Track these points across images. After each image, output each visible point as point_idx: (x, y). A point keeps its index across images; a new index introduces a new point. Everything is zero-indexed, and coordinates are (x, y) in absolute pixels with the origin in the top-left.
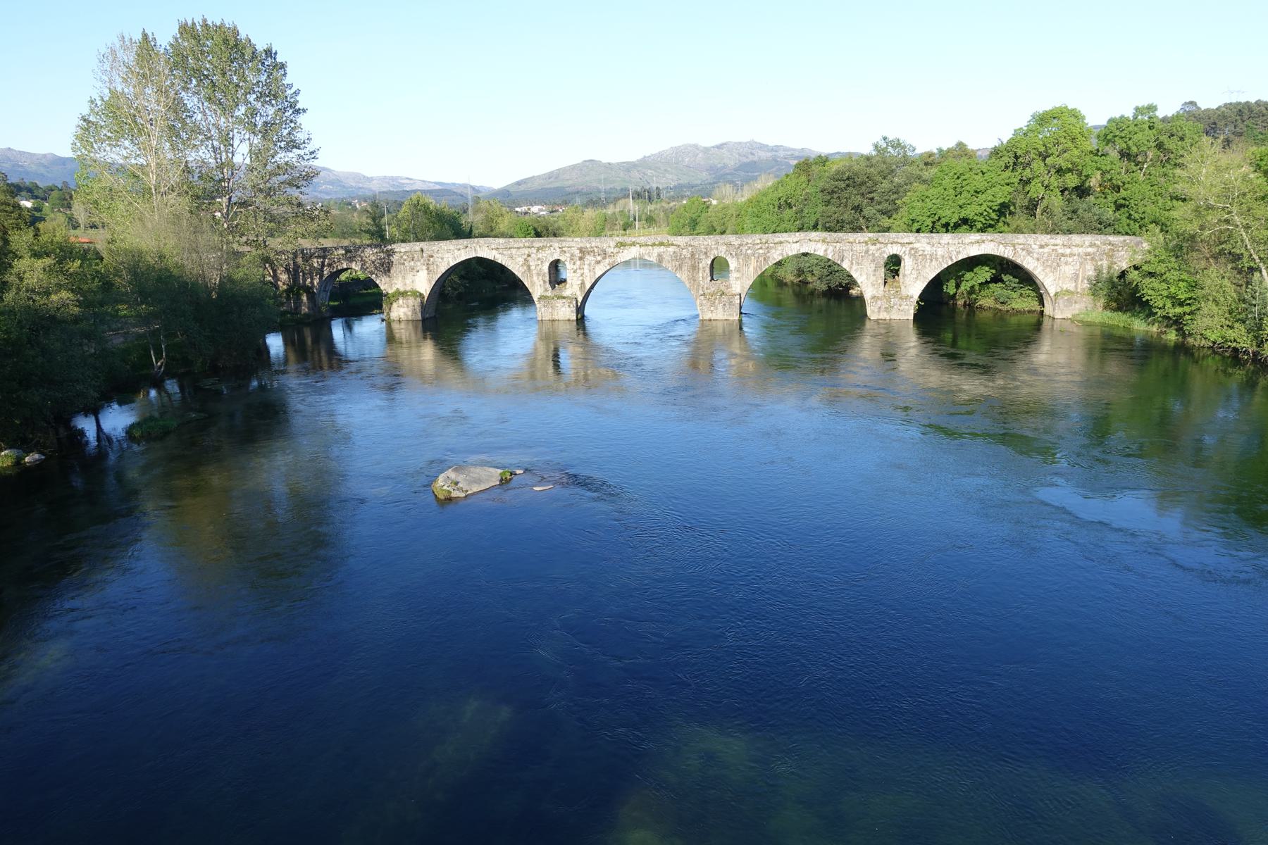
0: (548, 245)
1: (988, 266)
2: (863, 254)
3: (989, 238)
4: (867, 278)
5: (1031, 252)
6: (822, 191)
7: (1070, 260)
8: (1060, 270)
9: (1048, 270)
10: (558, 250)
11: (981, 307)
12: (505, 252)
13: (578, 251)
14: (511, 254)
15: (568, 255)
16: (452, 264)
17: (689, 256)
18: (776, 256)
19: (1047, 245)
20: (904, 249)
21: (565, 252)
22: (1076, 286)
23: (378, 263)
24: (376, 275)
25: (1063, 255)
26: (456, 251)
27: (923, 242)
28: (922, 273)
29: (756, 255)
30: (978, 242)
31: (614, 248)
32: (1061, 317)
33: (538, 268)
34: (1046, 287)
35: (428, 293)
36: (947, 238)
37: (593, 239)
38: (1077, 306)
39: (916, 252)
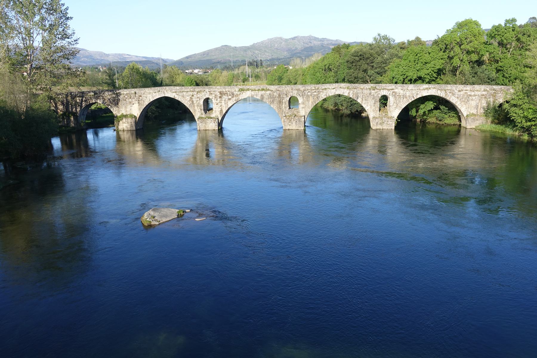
0: (203, 90)
1: (432, 101)
2: (368, 95)
3: (433, 87)
4: (370, 107)
5: (454, 94)
6: (347, 62)
7: (474, 98)
8: (469, 103)
9: (463, 103)
10: (208, 93)
11: (429, 122)
12: (180, 94)
13: (219, 94)
14: (183, 95)
15: (213, 95)
16: (152, 100)
17: (277, 96)
18: (323, 96)
19: (462, 91)
20: (389, 92)
21: (212, 94)
22: (477, 111)
23: (112, 100)
24: (111, 106)
25: (470, 95)
26: (154, 93)
27: (399, 89)
28: (399, 105)
29: (313, 96)
30: (427, 89)
31: (238, 92)
32: (470, 128)
33: (198, 102)
34: (462, 112)
35: (139, 115)
36: (411, 86)
37: (227, 87)
38: (478, 122)
39: (395, 94)
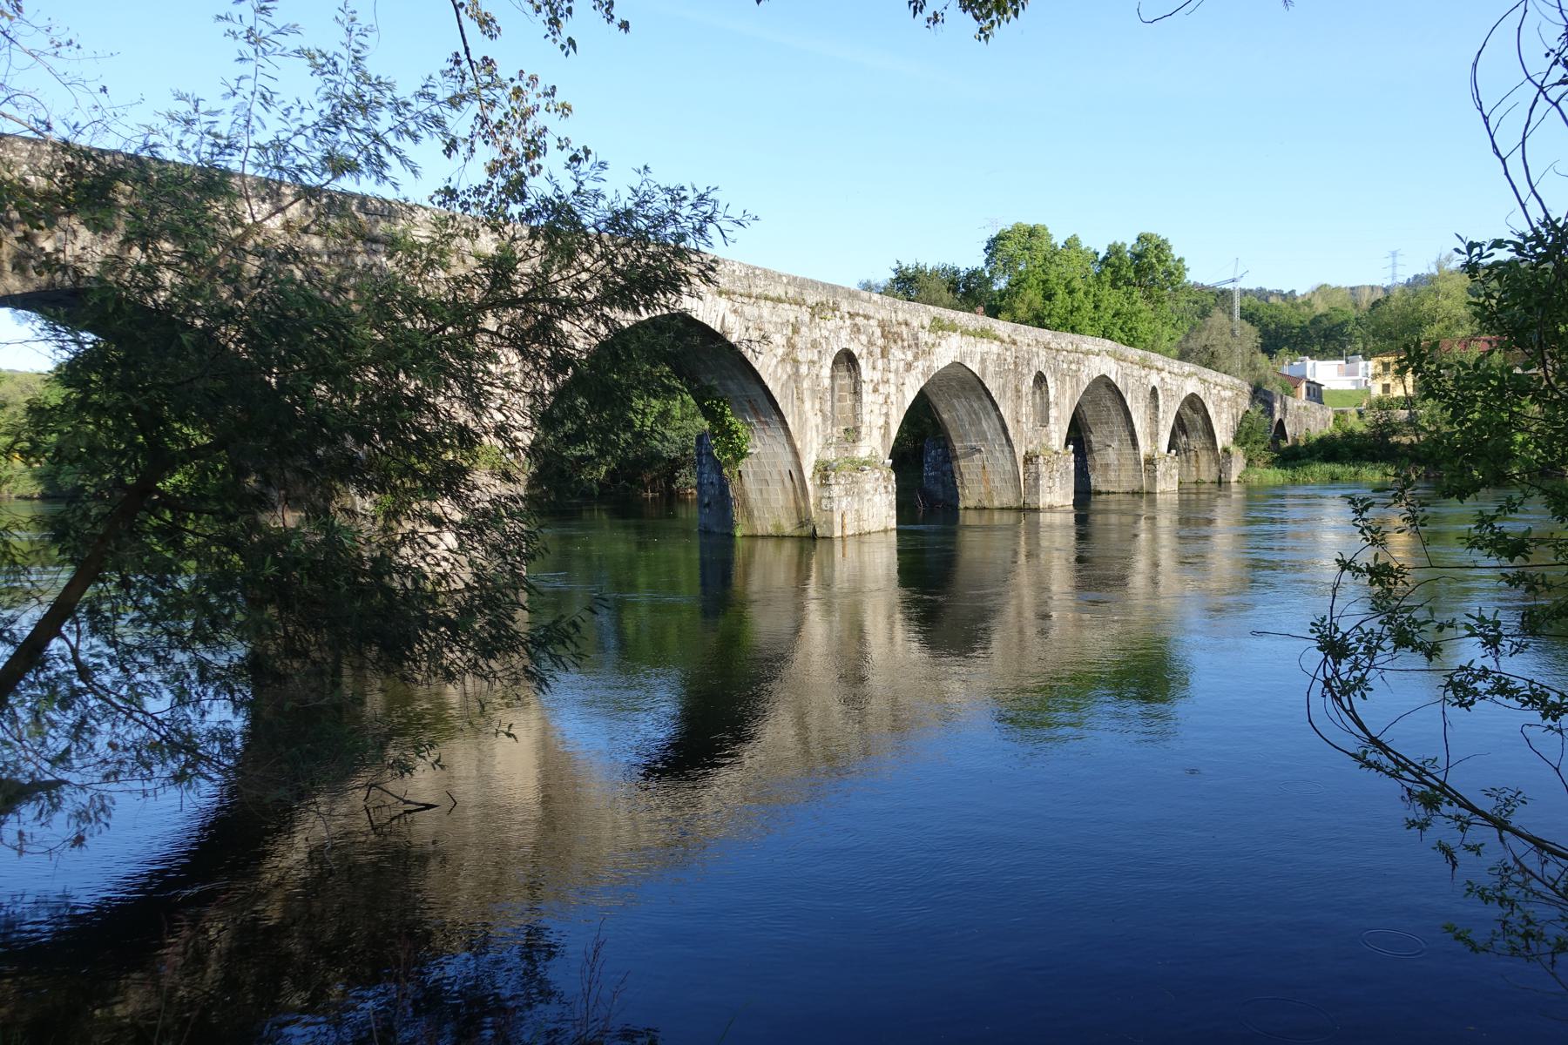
14: (760, 317)
15: (864, 339)
17: (1012, 367)
